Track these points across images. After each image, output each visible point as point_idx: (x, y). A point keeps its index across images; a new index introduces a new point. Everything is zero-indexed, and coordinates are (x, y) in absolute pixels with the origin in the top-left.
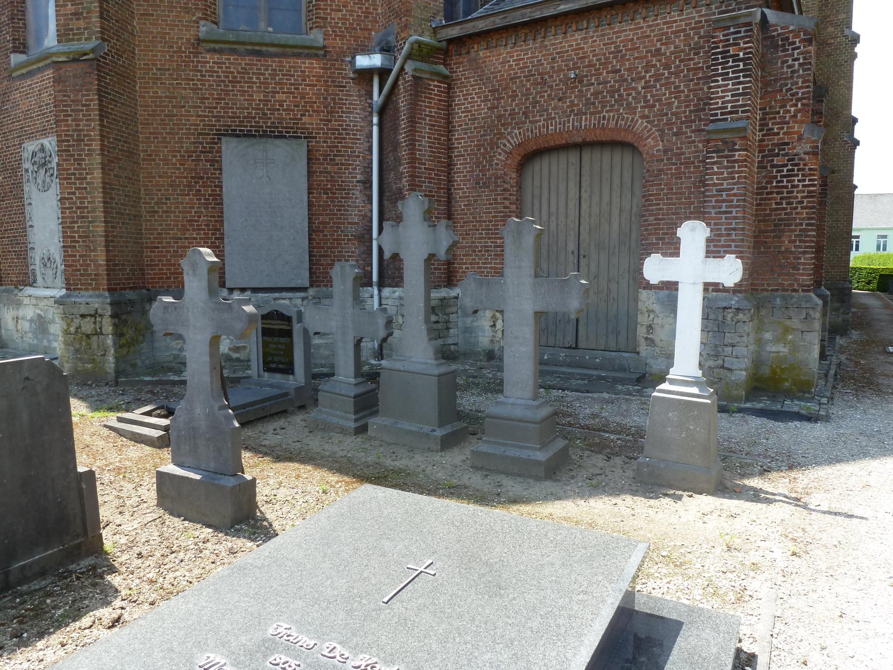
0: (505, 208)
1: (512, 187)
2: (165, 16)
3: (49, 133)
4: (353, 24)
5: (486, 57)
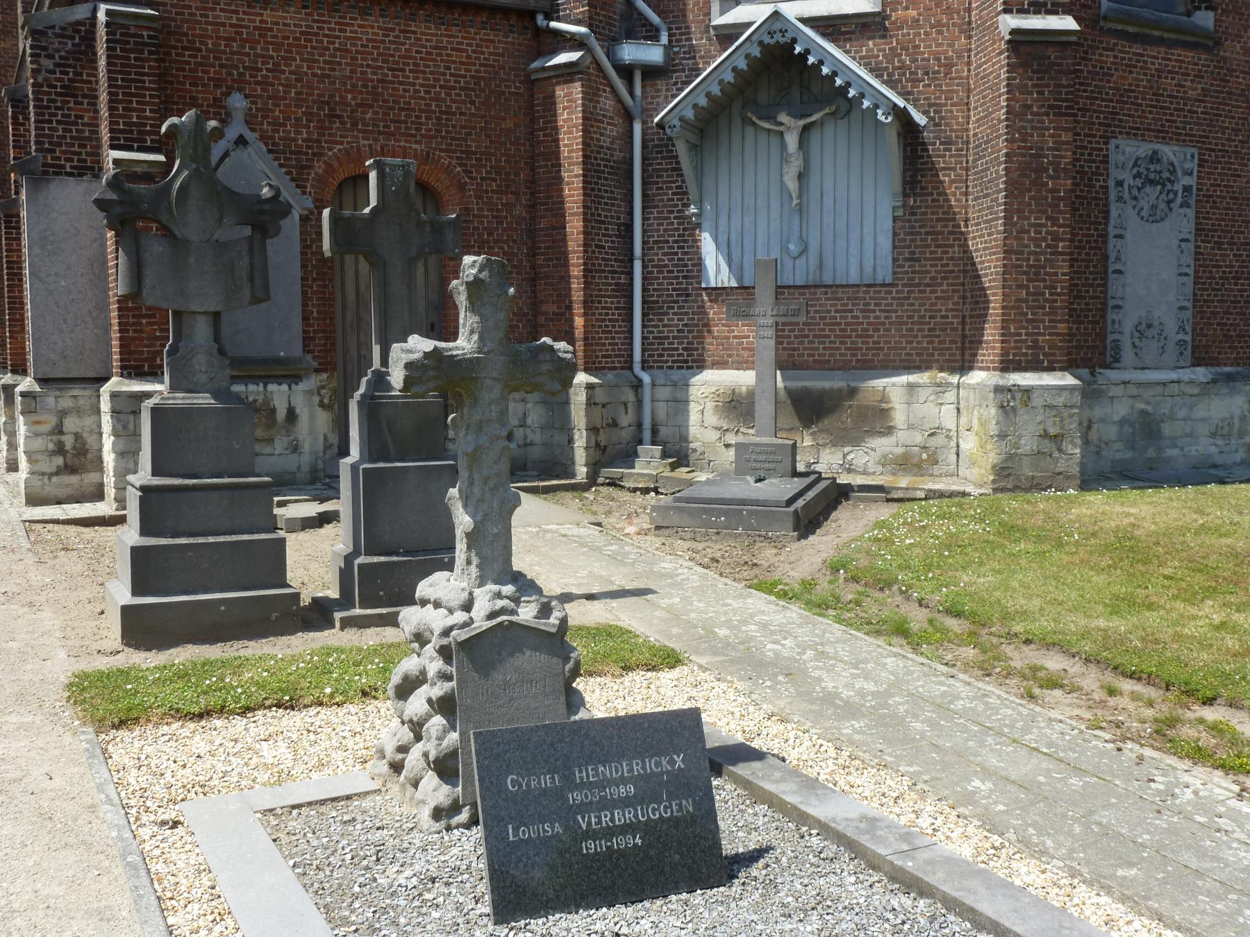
3: (1171, 139)
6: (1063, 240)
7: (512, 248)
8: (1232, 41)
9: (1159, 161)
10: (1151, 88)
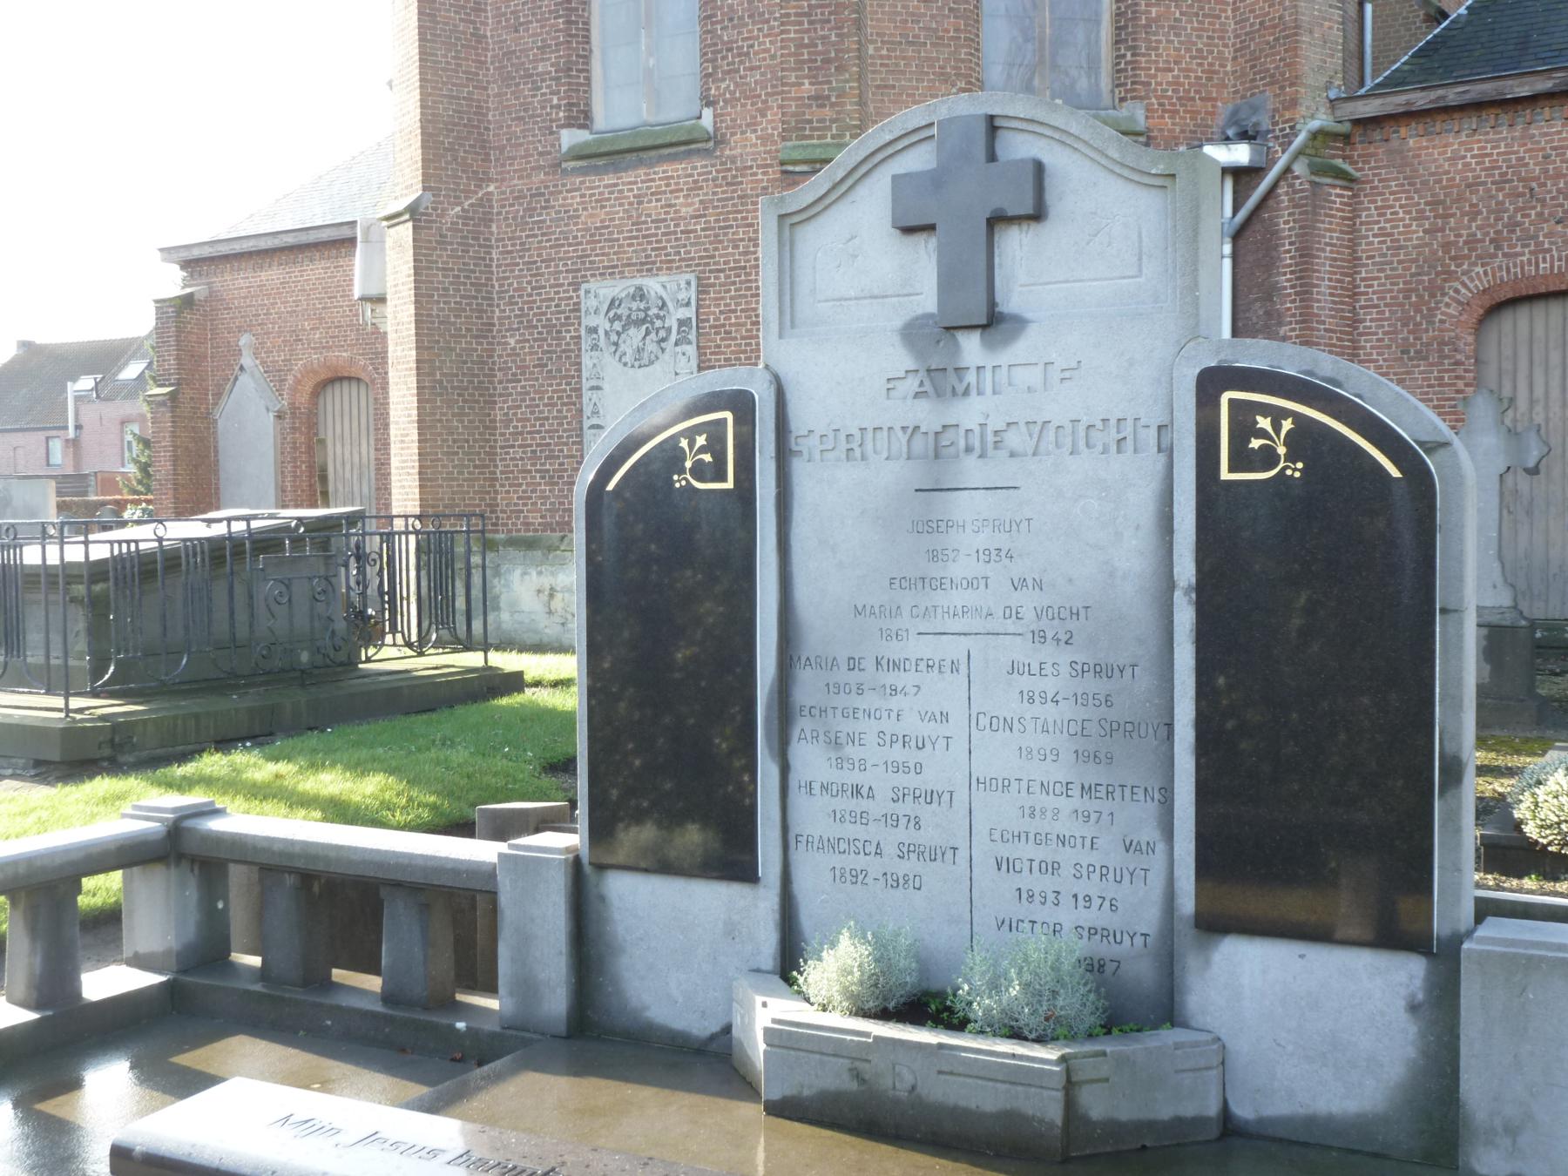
0: (1458, 392)
1: (1468, 358)
2: (913, 88)
3: (659, 269)
4: (1189, 91)
5: (1420, 148)
8: (743, 133)
9: (642, 297)
10: (630, 217)
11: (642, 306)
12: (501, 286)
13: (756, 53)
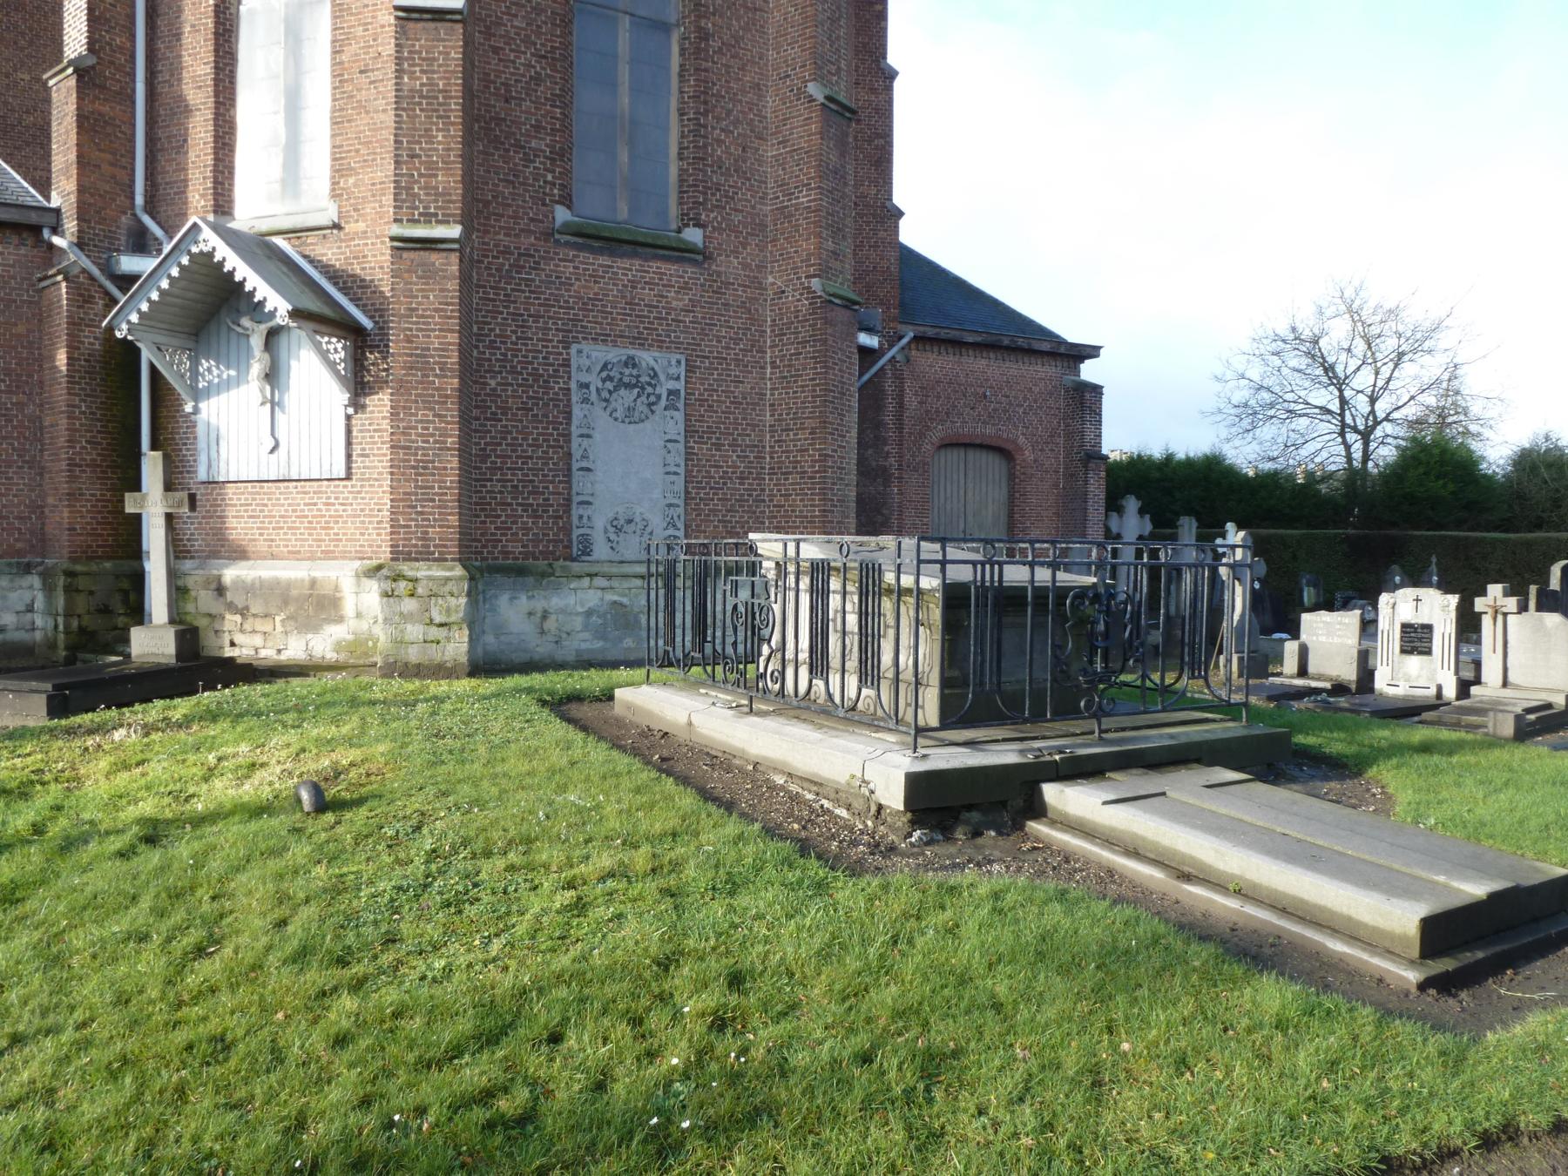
3: (652, 346)
6: (451, 436)
7: (24, 444)
8: (727, 256)
9: (634, 366)
10: (623, 297)
11: (635, 372)
12: (479, 329)
13: (739, 200)
